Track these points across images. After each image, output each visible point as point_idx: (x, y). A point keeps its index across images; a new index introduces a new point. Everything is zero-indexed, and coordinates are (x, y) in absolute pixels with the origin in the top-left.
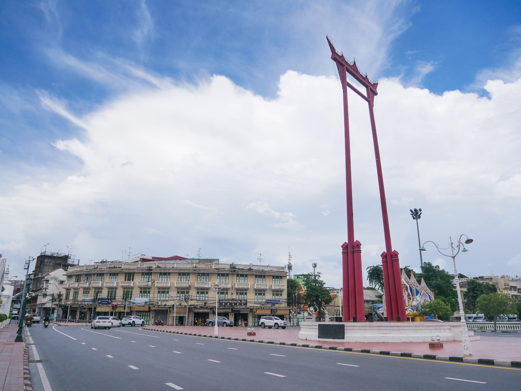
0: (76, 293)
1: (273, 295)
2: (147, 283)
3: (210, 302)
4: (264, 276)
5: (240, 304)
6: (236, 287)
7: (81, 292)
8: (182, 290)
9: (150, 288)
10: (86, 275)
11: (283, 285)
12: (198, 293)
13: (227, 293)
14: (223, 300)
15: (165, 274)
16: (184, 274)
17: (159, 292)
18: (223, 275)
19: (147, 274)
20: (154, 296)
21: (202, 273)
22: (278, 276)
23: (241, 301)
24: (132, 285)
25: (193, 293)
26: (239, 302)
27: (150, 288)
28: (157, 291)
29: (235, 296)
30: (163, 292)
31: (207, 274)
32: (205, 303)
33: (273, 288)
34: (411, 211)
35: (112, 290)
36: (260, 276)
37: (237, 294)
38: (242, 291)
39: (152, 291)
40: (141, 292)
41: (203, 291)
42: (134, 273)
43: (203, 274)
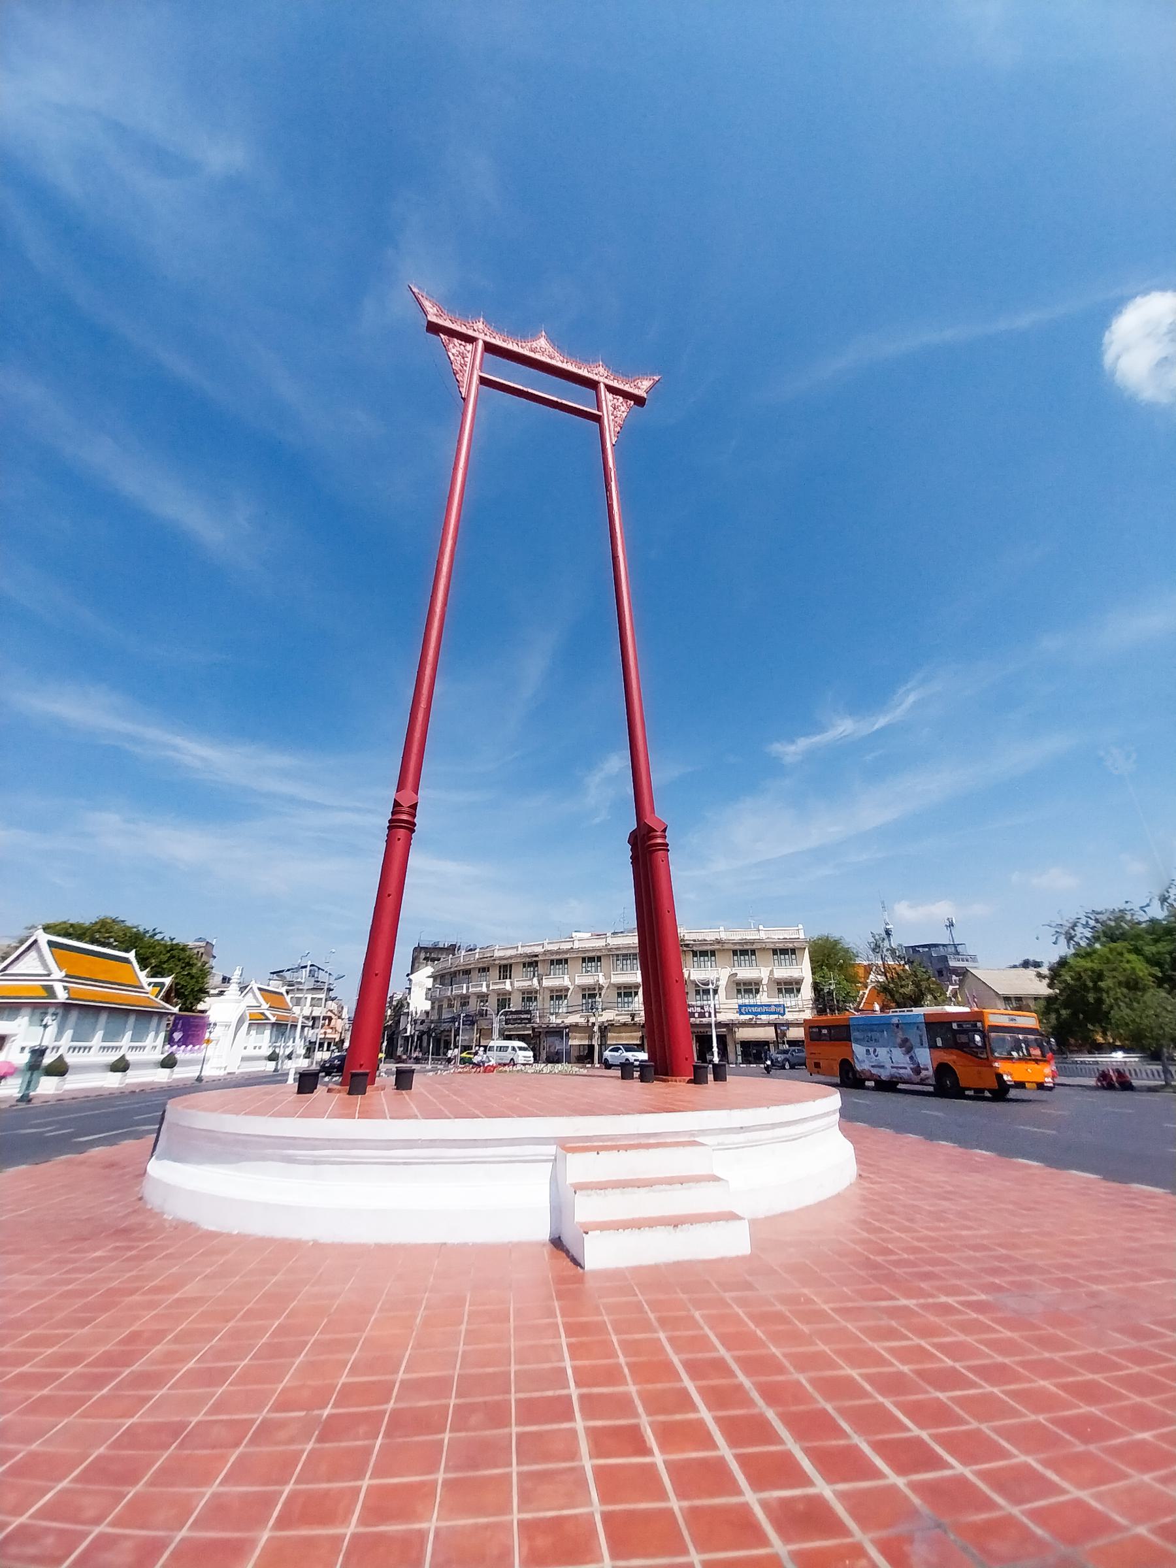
0: (440, 1007)
2: (529, 983)
4: (753, 952)
8: (590, 994)
10: (450, 974)
12: (619, 995)
15: (559, 962)
16: (591, 959)
17: (552, 998)
19: (530, 964)
21: (626, 955)
23: (702, 1007)
25: (609, 996)
26: (699, 1010)
32: (633, 1016)
35: (483, 998)
36: (744, 952)
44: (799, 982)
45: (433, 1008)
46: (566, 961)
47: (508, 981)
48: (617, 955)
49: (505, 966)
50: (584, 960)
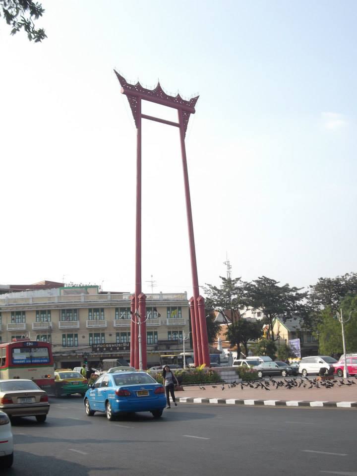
1: (169, 333)
3: (80, 348)
13: (103, 335)
14: (97, 344)
21: (68, 310)
26: (119, 345)
33: (168, 324)
41: (71, 334)
46: (24, 313)
50: (37, 312)
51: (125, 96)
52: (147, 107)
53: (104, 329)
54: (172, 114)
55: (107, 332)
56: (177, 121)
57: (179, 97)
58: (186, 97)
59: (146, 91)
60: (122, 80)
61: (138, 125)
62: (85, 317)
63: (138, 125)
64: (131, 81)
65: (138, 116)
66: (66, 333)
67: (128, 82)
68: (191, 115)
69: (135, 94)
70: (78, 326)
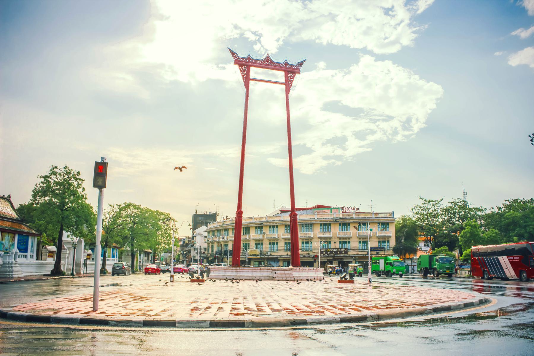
0: (213, 247)
1: (379, 242)
3: (314, 251)
5: (341, 252)
6: (338, 236)
7: (215, 245)
9: (262, 240)
11: (391, 232)
17: (270, 244)
18: (325, 225)
19: (259, 227)
20: (266, 247)
21: (306, 224)
22: (384, 223)
24: (248, 238)
27: (262, 240)
28: (268, 242)
29: (337, 245)
30: (273, 244)
31: (311, 224)
33: (377, 235)
34: (530, 136)
37: (340, 242)
38: (345, 241)
39: (264, 243)
40: (256, 244)
42: (249, 227)
43: (306, 225)
44: (389, 237)
45: (208, 246)
46: (277, 226)
47: (248, 236)
48: (302, 225)
49: (246, 228)
50: (286, 226)
51: (237, 67)
52: (254, 72)
53: (330, 238)
54: (280, 76)
55: (333, 241)
56: (283, 80)
57: (286, 63)
58: (293, 61)
59: (256, 61)
60: (233, 54)
61: (247, 86)
62: (266, 230)
63: (247, 86)
64: (242, 54)
65: (247, 79)
66: (304, 241)
67: (240, 55)
68: (297, 75)
69: (245, 64)
70: (312, 236)
